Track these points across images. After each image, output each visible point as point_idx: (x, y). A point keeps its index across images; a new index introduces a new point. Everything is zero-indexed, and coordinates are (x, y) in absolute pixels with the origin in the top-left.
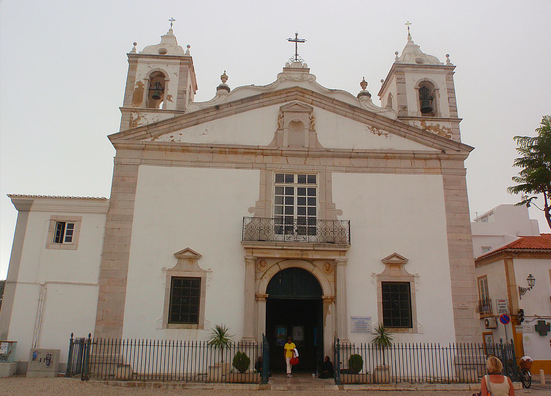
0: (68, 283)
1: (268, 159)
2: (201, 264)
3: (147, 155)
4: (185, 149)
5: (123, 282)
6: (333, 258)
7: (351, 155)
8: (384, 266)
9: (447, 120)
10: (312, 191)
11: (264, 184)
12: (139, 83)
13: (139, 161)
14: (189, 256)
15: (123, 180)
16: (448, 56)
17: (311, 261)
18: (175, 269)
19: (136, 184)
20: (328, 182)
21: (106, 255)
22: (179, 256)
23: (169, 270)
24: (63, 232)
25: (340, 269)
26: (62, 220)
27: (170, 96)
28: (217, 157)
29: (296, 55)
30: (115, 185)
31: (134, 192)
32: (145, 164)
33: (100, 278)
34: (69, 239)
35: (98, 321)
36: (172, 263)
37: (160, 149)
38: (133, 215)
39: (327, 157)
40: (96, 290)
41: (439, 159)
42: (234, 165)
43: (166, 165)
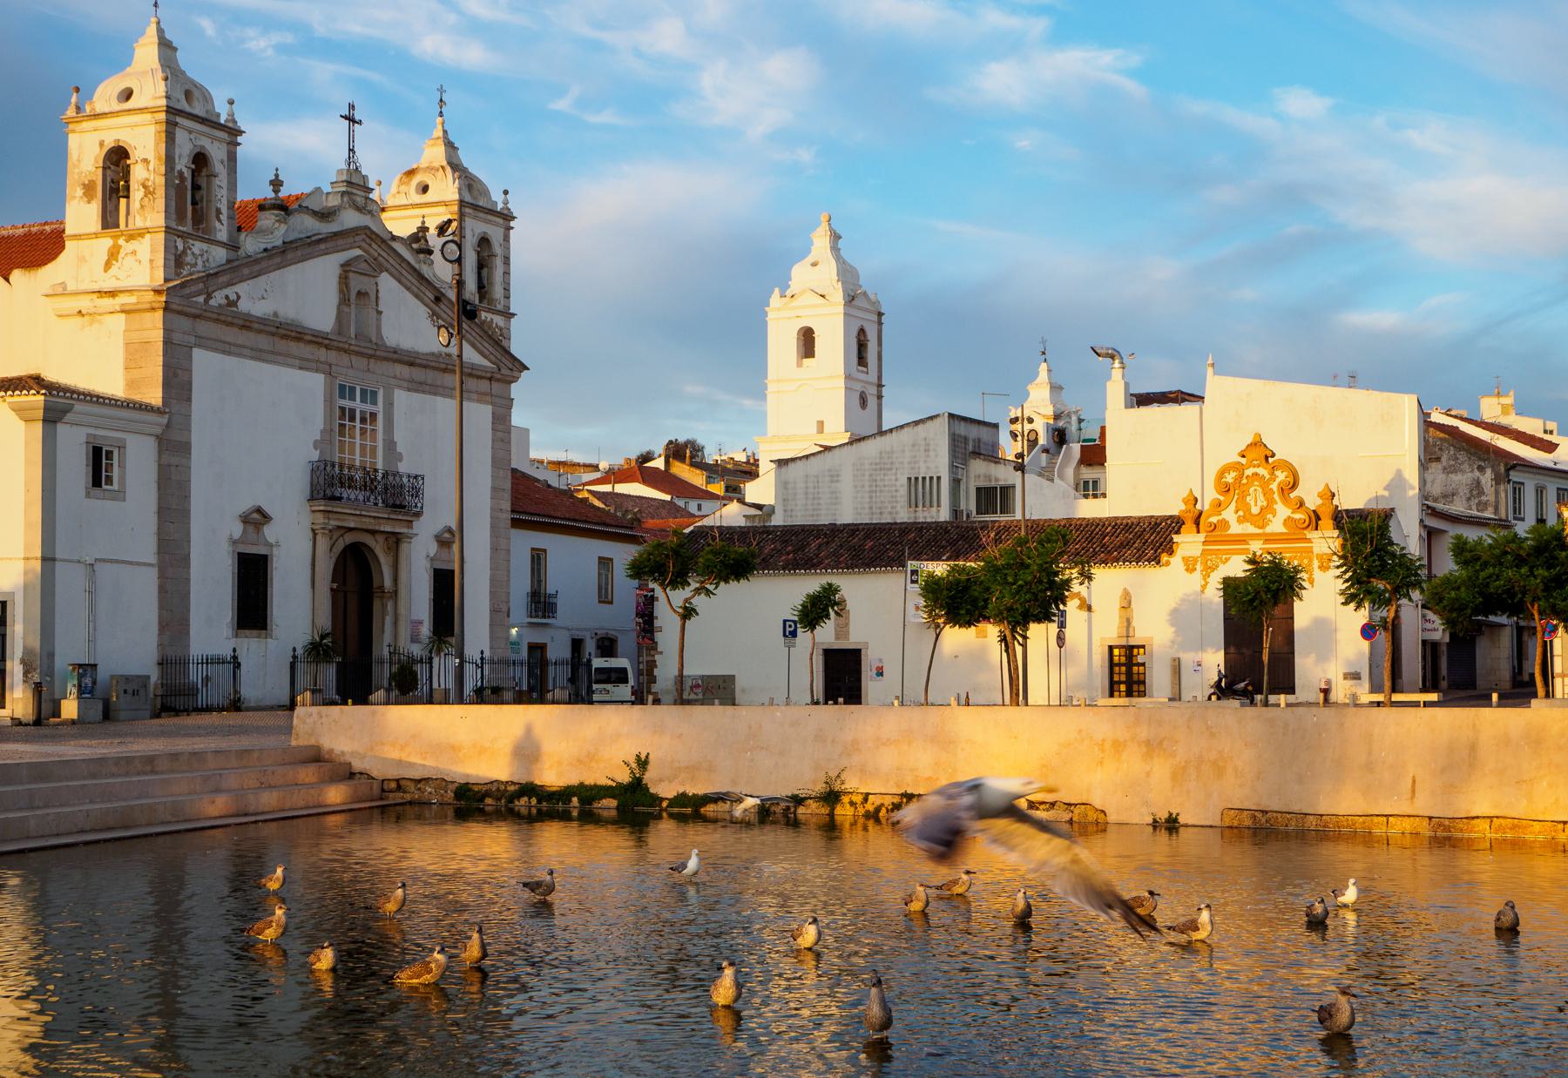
0: (117, 561)
1: (332, 356)
2: (269, 532)
3: (205, 328)
4: (247, 323)
5: (185, 561)
6: (397, 530)
7: (410, 360)
9: (499, 313)
10: (373, 416)
11: (329, 401)
12: (181, 173)
13: (192, 340)
14: (257, 519)
15: (175, 375)
16: (506, 192)
17: (373, 532)
18: (242, 540)
19: (190, 383)
20: (389, 405)
21: (163, 511)
22: (245, 519)
23: (235, 542)
24: (99, 464)
25: (404, 547)
26: (98, 443)
27: (219, 212)
28: (282, 345)
29: (351, 150)
30: (166, 385)
31: (189, 400)
32: (200, 346)
34: (109, 480)
35: (163, 626)
36: (237, 530)
37: (217, 321)
40: (153, 574)
41: (490, 379)
43: (224, 352)
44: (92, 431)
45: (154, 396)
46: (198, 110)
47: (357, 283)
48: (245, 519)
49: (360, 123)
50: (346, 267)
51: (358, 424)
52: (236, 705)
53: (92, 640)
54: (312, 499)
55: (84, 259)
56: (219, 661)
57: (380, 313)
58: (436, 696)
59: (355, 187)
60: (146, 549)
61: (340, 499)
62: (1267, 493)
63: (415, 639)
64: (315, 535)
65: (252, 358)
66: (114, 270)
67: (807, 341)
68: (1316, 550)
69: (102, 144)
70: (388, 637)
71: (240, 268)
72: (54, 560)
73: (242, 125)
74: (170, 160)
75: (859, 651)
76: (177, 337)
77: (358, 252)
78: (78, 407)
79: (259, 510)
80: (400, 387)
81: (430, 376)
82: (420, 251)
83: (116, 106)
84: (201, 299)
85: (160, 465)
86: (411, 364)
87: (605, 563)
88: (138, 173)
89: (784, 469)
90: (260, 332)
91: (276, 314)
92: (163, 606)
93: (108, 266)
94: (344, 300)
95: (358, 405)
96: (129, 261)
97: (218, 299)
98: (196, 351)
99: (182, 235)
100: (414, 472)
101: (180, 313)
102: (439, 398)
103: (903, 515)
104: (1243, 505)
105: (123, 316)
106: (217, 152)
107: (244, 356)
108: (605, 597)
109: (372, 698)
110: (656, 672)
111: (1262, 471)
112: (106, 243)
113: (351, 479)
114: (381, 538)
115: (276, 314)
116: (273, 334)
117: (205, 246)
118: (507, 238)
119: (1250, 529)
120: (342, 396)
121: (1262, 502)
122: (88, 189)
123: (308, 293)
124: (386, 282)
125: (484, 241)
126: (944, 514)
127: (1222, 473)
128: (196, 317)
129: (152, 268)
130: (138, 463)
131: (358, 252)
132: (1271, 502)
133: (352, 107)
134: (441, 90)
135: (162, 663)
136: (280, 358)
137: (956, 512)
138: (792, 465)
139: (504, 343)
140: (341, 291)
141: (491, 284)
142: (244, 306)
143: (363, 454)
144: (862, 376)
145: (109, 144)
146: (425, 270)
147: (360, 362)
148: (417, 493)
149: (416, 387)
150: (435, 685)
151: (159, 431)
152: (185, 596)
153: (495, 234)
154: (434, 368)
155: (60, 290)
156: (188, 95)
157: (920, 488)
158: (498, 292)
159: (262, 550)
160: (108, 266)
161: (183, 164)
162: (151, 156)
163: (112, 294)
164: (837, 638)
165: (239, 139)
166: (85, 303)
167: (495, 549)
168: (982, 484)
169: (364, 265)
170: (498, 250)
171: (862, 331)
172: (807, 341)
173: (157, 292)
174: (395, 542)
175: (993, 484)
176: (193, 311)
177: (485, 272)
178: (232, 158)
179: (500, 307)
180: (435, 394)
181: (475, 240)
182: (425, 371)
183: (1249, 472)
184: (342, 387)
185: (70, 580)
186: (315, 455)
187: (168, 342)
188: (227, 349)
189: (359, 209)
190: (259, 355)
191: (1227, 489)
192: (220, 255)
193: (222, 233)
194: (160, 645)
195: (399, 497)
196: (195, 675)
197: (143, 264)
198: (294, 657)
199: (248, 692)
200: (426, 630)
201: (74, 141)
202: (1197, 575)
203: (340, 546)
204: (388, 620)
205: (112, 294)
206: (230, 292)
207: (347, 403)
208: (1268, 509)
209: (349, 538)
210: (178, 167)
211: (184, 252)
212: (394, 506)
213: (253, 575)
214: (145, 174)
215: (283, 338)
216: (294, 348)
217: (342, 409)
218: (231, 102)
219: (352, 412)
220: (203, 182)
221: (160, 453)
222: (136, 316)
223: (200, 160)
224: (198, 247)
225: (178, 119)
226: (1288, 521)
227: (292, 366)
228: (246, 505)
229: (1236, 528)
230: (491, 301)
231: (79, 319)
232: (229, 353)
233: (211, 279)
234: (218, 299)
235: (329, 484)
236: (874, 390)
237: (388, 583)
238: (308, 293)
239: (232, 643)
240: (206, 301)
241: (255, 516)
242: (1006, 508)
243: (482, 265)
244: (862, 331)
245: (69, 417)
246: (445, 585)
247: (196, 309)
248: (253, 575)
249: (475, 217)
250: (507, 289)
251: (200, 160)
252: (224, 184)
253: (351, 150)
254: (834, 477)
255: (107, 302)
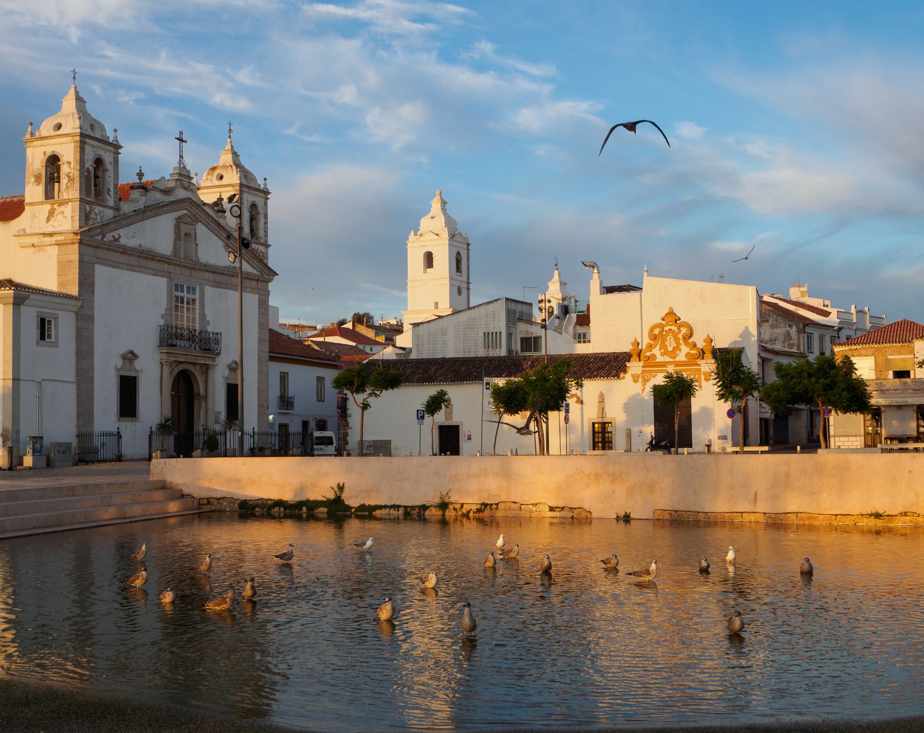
0: (54, 381)
1: (171, 268)
2: (137, 364)
3: (101, 253)
4: (125, 251)
5: (91, 380)
7: (214, 270)
8: (228, 370)
10: (194, 300)
11: (169, 293)
12: (88, 169)
13: (95, 260)
14: (130, 357)
16: (265, 179)
20: (202, 295)
21: (79, 353)
22: (124, 357)
23: (118, 370)
25: (210, 372)
27: (109, 190)
28: (143, 262)
29: (181, 157)
31: (93, 292)
32: (99, 263)
33: (77, 375)
34: (49, 336)
35: (79, 416)
36: (120, 363)
38: (93, 316)
39: (200, 270)
41: (257, 280)
42: (152, 272)
43: (112, 266)
44: (39, 309)
45: (74, 290)
46: (98, 135)
47: (184, 229)
48: (124, 357)
49: (186, 142)
50: (179, 220)
51: (185, 305)
52: (119, 459)
53: (40, 424)
54: (160, 346)
55: (35, 217)
56: (110, 434)
57: (197, 245)
58: (229, 453)
59: (184, 177)
60: (70, 374)
61: (176, 346)
62: (677, 340)
63: (217, 421)
64: (162, 365)
65: (127, 270)
66: (51, 222)
67: (429, 259)
68: (703, 370)
69: (45, 153)
70: (202, 421)
71: (121, 220)
72: (19, 380)
73: (121, 143)
74: (82, 162)
75: (457, 427)
76: (86, 258)
77: (185, 212)
78: (32, 296)
79: (131, 352)
80: (209, 285)
81: (224, 279)
82: (219, 211)
83: (53, 133)
84: (99, 237)
85: (77, 328)
86: (214, 273)
87: (320, 380)
88: (64, 169)
89: (417, 328)
90: (131, 255)
91: (140, 246)
92: (79, 404)
93: (48, 219)
94: (178, 238)
95: (185, 295)
96: (60, 217)
97: (109, 237)
98: (97, 267)
99: (89, 203)
100: (216, 331)
101: (87, 245)
102: (230, 292)
103: (481, 353)
104: (663, 346)
105: (57, 247)
106: (108, 158)
107: (124, 269)
108: (320, 398)
109: (194, 454)
110: (348, 439)
111: (673, 328)
112: (48, 207)
113: (182, 335)
114: (198, 367)
115: (140, 246)
116: (139, 257)
117: (101, 209)
118: (266, 204)
119: (668, 359)
120: (177, 290)
121: (674, 344)
122: (38, 178)
123: (159, 234)
124: (201, 229)
125: (254, 206)
126: (503, 352)
127: (652, 329)
128: (96, 247)
129: (72, 221)
130: (65, 327)
131: (185, 212)
132: (678, 344)
133: (181, 133)
134: (230, 124)
135: (79, 436)
136: (142, 269)
137: (510, 351)
138: (421, 326)
139: (265, 261)
140: (176, 233)
141: (258, 229)
142: (123, 241)
143: (188, 321)
144: (459, 278)
145: (49, 153)
146: (222, 221)
147: (187, 272)
148: (218, 342)
149: (217, 285)
150: (228, 447)
151: (76, 309)
152: (92, 399)
153: (259, 201)
154: (227, 275)
155: (22, 233)
156: (92, 127)
157: (490, 338)
158: (261, 233)
159: (133, 374)
160: (48, 219)
161: (89, 165)
162: (72, 160)
163: (51, 235)
164: (446, 419)
165: (120, 151)
166: (36, 240)
167: (260, 372)
168: (523, 336)
169: (189, 219)
170: (261, 210)
171: (458, 254)
172: (429, 259)
173: (76, 234)
174: (206, 369)
175: (530, 336)
176: (95, 244)
177: (254, 222)
178: (116, 161)
179: (262, 241)
180: (227, 289)
181: (249, 205)
182: (222, 276)
183: (667, 328)
184: (176, 285)
185: (28, 391)
186: (162, 322)
187: (81, 261)
188: (114, 264)
189: (186, 189)
190: (131, 268)
191: (654, 338)
192: (109, 213)
193: (111, 202)
194: (78, 426)
195: (208, 345)
196: (97, 442)
197: (67, 219)
198: (151, 432)
199: (126, 451)
200: (223, 416)
201: (29, 151)
202: (639, 384)
203: (176, 371)
204: (202, 412)
205: (51, 235)
206: (116, 234)
207: (179, 294)
208: (677, 348)
209: (181, 367)
210: (86, 166)
211: (90, 212)
212: (206, 350)
213: (128, 388)
214: (69, 170)
215: (145, 259)
216: (151, 264)
217: (177, 297)
218: (115, 131)
219: (182, 298)
220: (100, 174)
221: (77, 320)
222: (64, 247)
223: (99, 162)
224: (98, 209)
225: (87, 140)
226: (687, 355)
227: (149, 274)
228: (124, 350)
229: (660, 359)
230: (257, 238)
231: (33, 249)
232: (115, 267)
233: (105, 227)
234: (109, 237)
235: (169, 338)
236: (465, 285)
237: (202, 392)
238: (159, 234)
239: (117, 425)
240: (102, 239)
241: (130, 355)
242: (537, 348)
243: (252, 219)
244: (458, 254)
245: (27, 302)
246: (233, 392)
247: (96, 243)
248: (128, 388)
249: (249, 193)
250: (266, 232)
251: (99, 162)
252: (112, 175)
253: (181, 157)
254: (444, 332)
255: (48, 240)
